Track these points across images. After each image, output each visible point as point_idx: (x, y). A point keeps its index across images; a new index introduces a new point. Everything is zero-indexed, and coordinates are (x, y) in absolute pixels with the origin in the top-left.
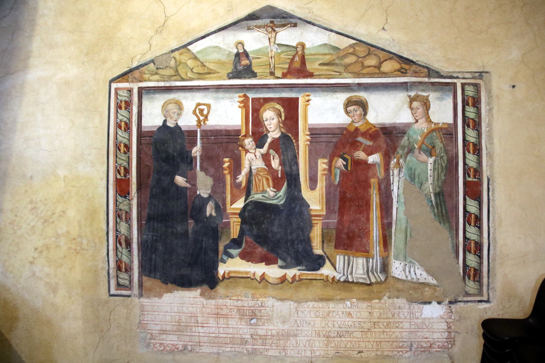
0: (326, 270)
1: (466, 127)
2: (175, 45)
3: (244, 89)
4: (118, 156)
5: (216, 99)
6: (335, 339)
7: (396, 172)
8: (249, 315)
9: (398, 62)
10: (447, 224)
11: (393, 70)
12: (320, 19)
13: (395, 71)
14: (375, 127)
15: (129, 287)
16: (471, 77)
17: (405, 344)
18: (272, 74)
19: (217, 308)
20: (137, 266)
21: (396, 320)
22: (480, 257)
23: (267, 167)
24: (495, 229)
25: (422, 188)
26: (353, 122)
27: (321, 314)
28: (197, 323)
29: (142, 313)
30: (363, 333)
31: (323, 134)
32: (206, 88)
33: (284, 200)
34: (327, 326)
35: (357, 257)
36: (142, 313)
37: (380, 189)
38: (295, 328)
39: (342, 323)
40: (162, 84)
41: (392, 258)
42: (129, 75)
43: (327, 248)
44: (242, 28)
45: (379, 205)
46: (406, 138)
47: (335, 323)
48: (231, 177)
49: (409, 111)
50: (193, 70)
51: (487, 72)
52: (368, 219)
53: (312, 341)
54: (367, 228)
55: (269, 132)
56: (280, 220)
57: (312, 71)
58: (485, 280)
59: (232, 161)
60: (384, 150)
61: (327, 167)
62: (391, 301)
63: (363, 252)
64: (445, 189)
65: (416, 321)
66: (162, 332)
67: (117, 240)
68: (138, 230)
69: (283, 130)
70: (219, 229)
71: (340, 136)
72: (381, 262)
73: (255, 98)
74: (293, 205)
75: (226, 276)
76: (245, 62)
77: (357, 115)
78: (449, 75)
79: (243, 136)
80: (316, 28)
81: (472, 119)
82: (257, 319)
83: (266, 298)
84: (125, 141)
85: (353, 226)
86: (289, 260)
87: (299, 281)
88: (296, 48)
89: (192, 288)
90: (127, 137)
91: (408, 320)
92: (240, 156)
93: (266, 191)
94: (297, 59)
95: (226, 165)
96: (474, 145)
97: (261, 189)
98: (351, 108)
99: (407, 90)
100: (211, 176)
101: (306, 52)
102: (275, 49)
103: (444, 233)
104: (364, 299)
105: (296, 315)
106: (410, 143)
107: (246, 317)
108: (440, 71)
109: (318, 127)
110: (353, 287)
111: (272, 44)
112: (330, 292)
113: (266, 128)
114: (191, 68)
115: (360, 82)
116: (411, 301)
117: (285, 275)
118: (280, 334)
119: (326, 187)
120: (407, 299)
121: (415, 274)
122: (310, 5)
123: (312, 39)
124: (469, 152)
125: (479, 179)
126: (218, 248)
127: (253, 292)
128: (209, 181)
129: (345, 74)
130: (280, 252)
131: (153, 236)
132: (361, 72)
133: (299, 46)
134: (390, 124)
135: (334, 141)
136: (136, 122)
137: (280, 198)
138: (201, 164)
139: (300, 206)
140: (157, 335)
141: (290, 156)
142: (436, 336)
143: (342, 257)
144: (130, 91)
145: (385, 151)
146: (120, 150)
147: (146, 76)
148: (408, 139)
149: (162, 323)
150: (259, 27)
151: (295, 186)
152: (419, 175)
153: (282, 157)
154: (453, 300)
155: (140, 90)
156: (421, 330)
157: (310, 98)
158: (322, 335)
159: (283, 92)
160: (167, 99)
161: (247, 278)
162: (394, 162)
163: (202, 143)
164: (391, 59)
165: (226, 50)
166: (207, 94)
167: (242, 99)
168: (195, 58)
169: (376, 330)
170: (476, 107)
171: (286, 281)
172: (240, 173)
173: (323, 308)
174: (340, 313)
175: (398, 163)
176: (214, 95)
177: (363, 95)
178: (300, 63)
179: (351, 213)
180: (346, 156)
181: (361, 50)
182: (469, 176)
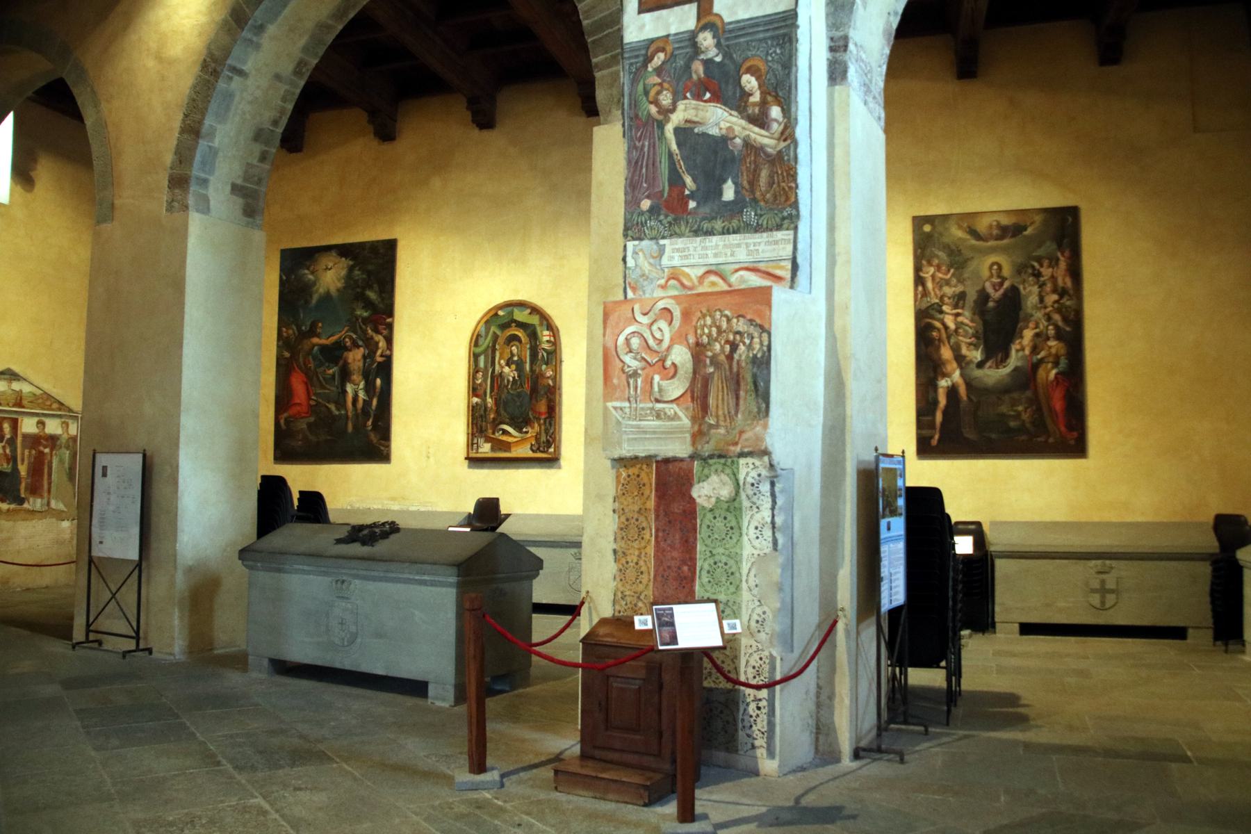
0: (26, 505)
123: (26, 388)
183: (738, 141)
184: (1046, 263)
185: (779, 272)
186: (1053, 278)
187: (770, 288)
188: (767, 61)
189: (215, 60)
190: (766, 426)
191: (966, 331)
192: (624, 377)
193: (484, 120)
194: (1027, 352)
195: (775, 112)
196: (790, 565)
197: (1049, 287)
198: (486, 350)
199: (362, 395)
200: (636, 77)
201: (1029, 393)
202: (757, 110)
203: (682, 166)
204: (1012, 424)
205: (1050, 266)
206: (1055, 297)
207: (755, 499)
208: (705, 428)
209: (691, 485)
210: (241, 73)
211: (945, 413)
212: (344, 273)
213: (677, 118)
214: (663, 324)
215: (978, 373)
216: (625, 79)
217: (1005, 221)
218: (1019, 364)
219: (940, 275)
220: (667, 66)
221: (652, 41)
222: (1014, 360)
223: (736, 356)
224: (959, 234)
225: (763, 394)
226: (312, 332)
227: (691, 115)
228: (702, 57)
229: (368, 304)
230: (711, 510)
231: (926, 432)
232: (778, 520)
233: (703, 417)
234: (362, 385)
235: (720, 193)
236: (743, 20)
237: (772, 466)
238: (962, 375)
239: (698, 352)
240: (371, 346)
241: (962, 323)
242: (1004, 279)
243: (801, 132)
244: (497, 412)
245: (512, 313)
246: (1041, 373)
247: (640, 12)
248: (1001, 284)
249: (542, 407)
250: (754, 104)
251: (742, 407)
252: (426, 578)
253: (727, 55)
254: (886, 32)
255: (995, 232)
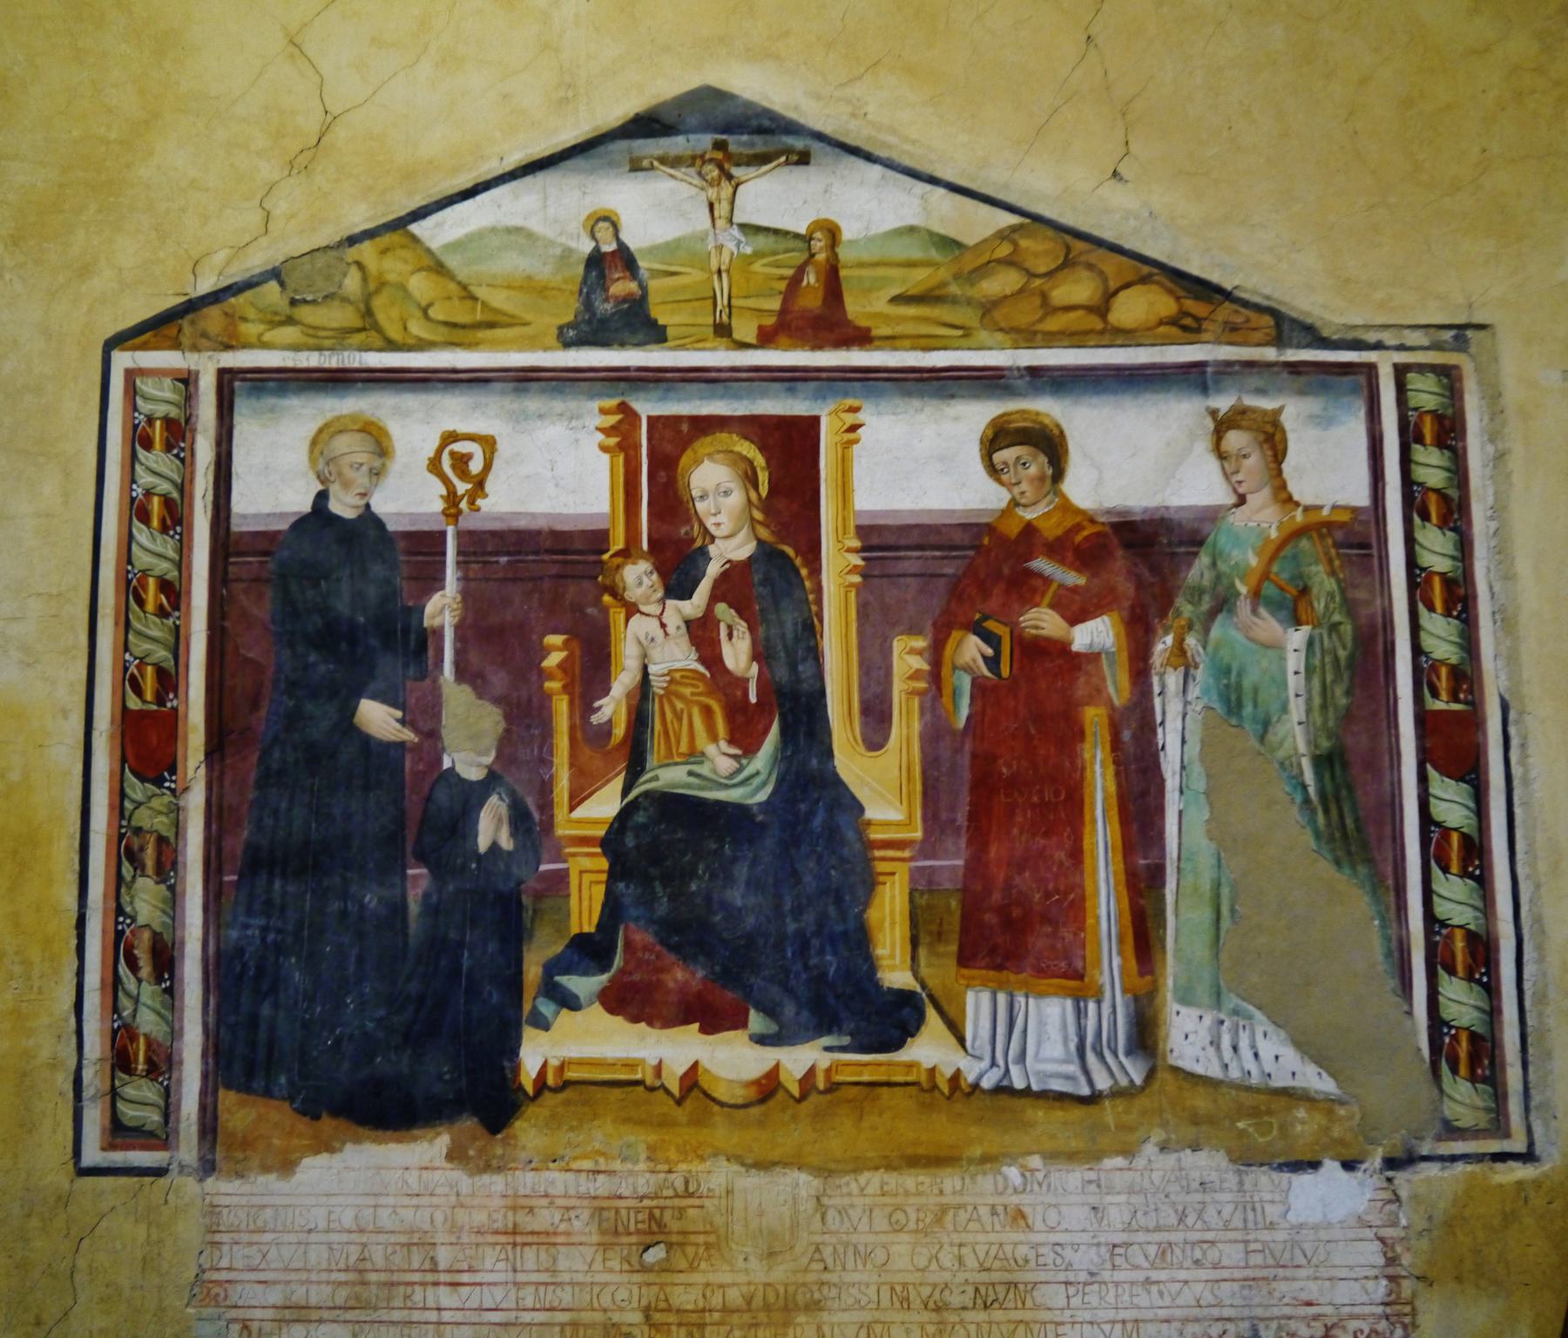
0: (929, 1050)
1: (1417, 520)
2: (360, 217)
3: (622, 385)
4: (135, 624)
5: (518, 418)
6: (970, 1316)
7: (1173, 680)
8: (638, 1232)
9: (1170, 292)
10: (1363, 870)
11: (1153, 319)
12: (891, 139)
13: (1161, 323)
14: (1092, 521)
15: (161, 1138)
16: (1425, 342)
17: (1230, 1326)
18: (723, 330)
19: (514, 1208)
20: (198, 1051)
21: (1194, 1236)
22: (1491, 990)
23: (708, 668)
24: (1538, 886)
25: (1270, 737)
26: (1014, 503)
27: (913, 1217)
28: (434, 1270)
29: (209, 1237)
30: (1072, 1290)
31: (908, 548)
32: (477, 379)
33: (769, 789)
34: (934, 1266)
35: (1041, 995)
36: (209, 1237)
37: (1116, 744)
38: (811, 1277)
39: (993, 1253)
40: (311, 360)
41: (1169, 996)
42: (185, 323)
43: (930, 965)
44: (612, 164)
45: (1114, 801)
46: (1204, 560)
47: (964, 1251)
48: (571, 703)
49: (1213, 464)
50: (431, 312)
51: (1481, 327)
52: (1077, 854)
53: (878, 1328)
54: (1072, 889)
55: (713, 538)
56: (754, 862)
57: (863, 323)
58: (1513, 1075)
59: (575, 645)
60: (1127, 604)
61: (926, 667)
62: (1170, 1160)
63: (1065, 976)
64: (1349, 741)
65: (1265, 1236)
66: (288, 1314)
67: (120, 946)
68: (206, 909)
69: (764, 533)
70: (526, 900)
71: (971, 553)
72: (1128, 1015)
73: (659, 418)
74: (803, 807)
75: (550, 1081)
76: (622, 287)
77: (1032, 480)
78: (1350, 336)
79: (617, 554)
80: (877, 170)
81: (1437, 491)
82: (670, 1246)
83: (702, 1159)
84: (163, 567)
85: (1024, 881)
86: (789, 1010)
87: (828, 1091)
88: (807, 239)
89: (416, 1132)
90: (171, 554)
91: (1238, 1235)
92: (608, 627)
93: (703, 754)
94: (811, 278)
95: (553, 660)
96: (1448, 582)
97: (684, 748)
98: (1005, 455)
99: (1204, 389)
100: (497, 701)
101: (844, 254)
102: (731, 241)
103: (1353, 902)
104: (1072, 1157)
105: (816, 1223)
106: (1218, 577)
107: (625, 1240)
108: (1318, 324)
109: (890, 522)
110: (1030, 1112)
111: (720, 223)
112: (941, 1129)
113: (701, 524)
114: (424, 303)
115: (1035, 363)
116: (1245, 1158)
117: (777, 1068)
118: (758, 1302)
119: (922, 738)
120: (1229, 1152)
121: (1256, 1055)
122: (857, 90)
123: (866, 210)
124: (1431, 609)
125: (1472, 704)
126: (519, 972)
127: (652, 1138)
128: (490, 720)
129: (983, 336)
130: (756, 982)
131: (265, 930)
132: (1040, 327)
133: (818, 235)
134: (1146, 510)
135: (949, 570)
136: (210, 497)
137: (757, 781)
138: (459, 654)
139: (830, 809)
140: (267, 1327)
141: (789, 626)
142: (1345, 1293)
143: (985, 997)
144: (187, 381)
145: (1133, 608)
146: (141, 603)
147: (251, 330)
148: (1214, 564)
149: (294, 1276)
150: (674, 162)
151: (811, 734)
152: (1256, 690)
153: (761, 631)
154: (1399, 1153)
155: (227, 381)
156: (1288, 1273)
157: (861, 417)
158: (916, 1303)
159: (764, 395)
160: (329, 416)
161: (627, 1089)
162: (1163, 644)
163: (465, 579)
164: (1144, 280)
165: (552, 243)
166: (483, 400)
167: (613, 419)
168: (438, 268)
169: (1119, 1276)
170: (1449, 448)
171: (780, 1095)
172: (606, 691)
173: (919, 1194)
174: (984, 1211)
175: (1180, 649)
176: (510, 403)
177: (1048, 408)
178: (820, 295)
179: (1015, 831)
180: (991, 625)
181: (1040, 251)
182: (1435, 694)
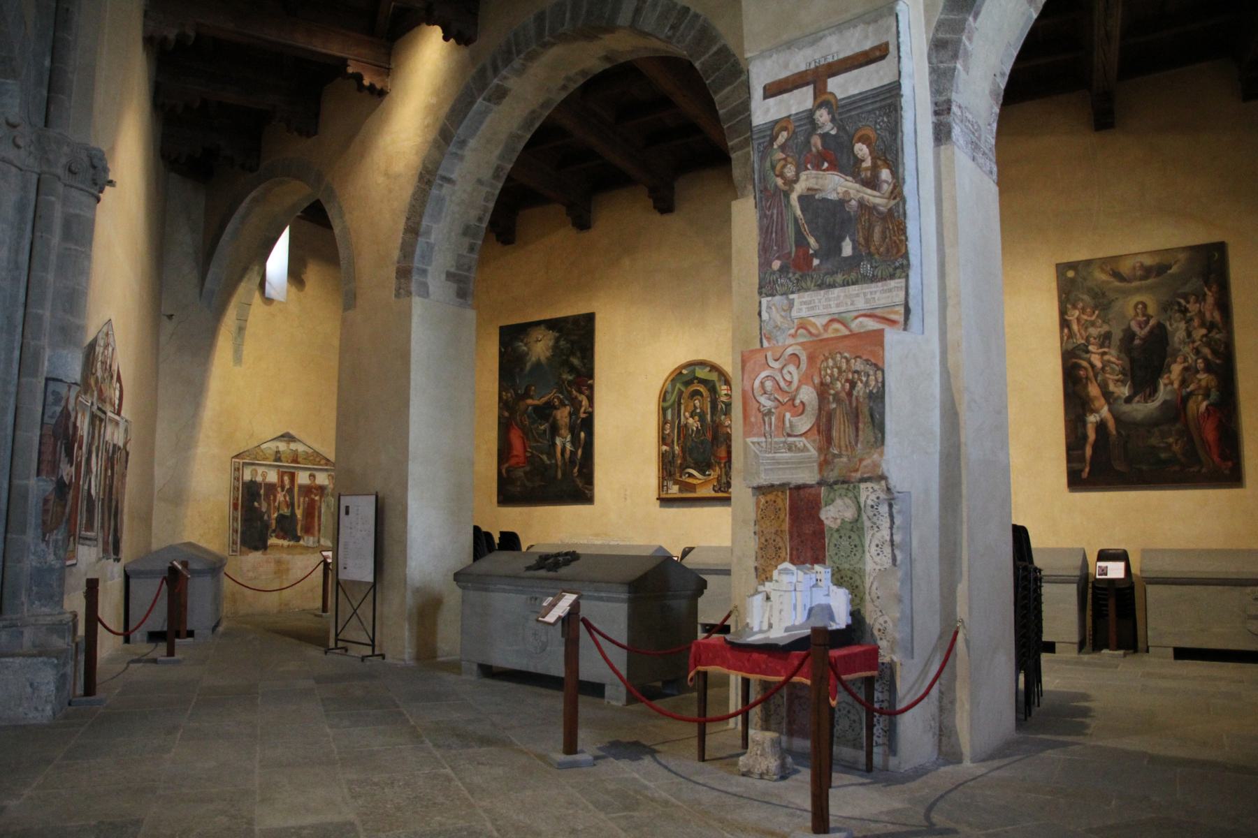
0: (301, 542)
183: (853, 203)
184: (1192, 299)
185: (893, 317)
186: (1201, 314)
187: (882, 331)
188: (876, 130)
189: (428, 172)
190: (882, 454)
191: (1113, 369)
192: (760, 415)
193: (665, 206)
194: (1176, 385)
195: (885, 174)
196: (909, 578)
197: (1196, 322)
198: (672, 406)
199: (569, 446)
200: (765, 153)
201: (1178, 426)
202: (869, 174)
203: (806, 228)
204: (1163, 456)
205: (1197, 301)
206: (1204, 331)
207: (875, 519)
208: (829, 457)
209: (819, 509)
210: (449, 181)
211: (1095, 447)
212: (551, 343)
213: (800, 188)
214: (792, 368)
215: (1126, 408)
216: (755, 157)
217: (1148, 261)
218: (1168, 398)
219: (1085, 317)
220: (790, 143)
221: (776, 122)
222: (1162, 394)
223: (855, 393)
224: (1104, 277)
225: (878, 425)
226: (527, 395)
227: (812, 183)
228: (819, 131)
229: (572, 369)
230: (838, 530)
231: (1076, 466)
232: (897, 538)
233: (828, 448)
234: (569, 438)
235: (840, 250)
236: (854, 96)
237: (888, 489)
238: (1110, 410)
239: (823, 391)
240: (576, 405)
241: (1109, 361)
242: (1149, 317)
243: (908, 189)
244: (684, 458)
245: (694, 372)
246: (1191, 405)
247: (765, 97)
248: (1147, 322)
249: (723, 454)
250: (867, 169)
251: (861, 439)
252: (603, 594)
253: (841, 128)
254: (993, 93)
255: (1139, 273)
